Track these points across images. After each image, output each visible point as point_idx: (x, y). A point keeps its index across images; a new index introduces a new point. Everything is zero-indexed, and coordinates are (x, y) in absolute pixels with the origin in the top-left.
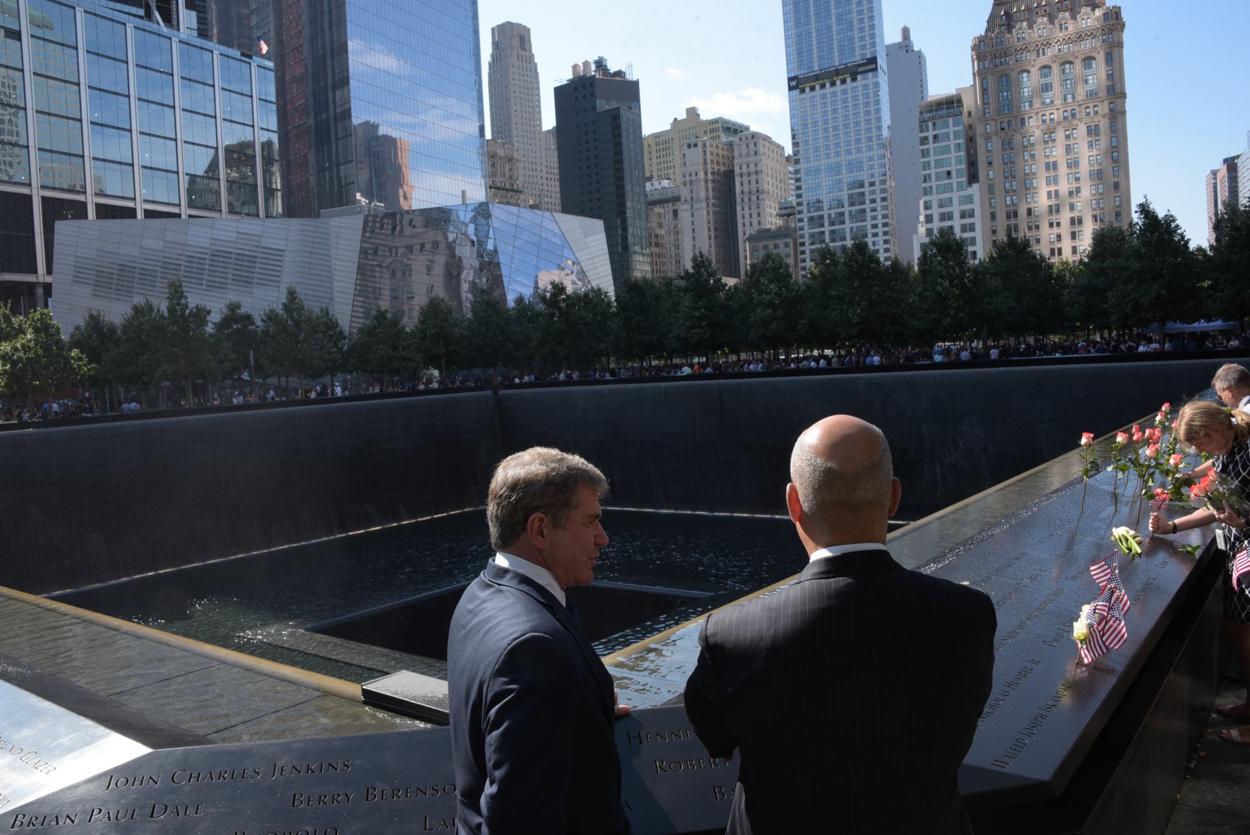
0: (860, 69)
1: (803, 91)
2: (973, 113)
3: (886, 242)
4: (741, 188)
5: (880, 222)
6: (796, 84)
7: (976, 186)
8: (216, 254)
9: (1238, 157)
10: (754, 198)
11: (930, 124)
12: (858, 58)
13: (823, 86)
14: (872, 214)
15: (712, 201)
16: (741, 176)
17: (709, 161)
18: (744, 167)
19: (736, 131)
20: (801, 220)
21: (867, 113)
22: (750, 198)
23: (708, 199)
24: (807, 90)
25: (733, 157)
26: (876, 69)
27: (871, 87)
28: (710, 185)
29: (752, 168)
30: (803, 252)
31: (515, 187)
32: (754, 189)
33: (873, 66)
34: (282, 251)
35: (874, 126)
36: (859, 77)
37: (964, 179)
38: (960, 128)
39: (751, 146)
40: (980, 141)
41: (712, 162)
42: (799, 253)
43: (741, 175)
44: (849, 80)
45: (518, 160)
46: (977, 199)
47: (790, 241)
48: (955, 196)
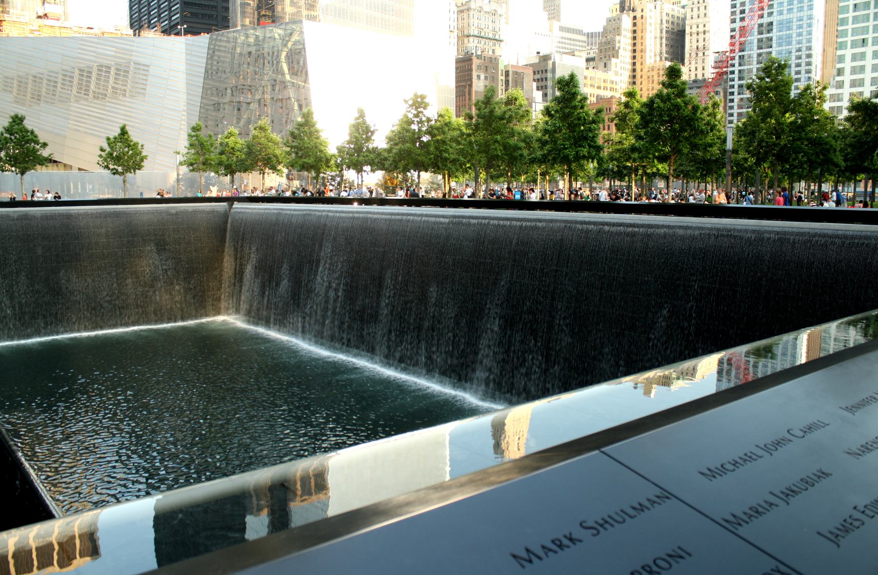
4: (690, 45)
8: (100, 67)
10: (700, 54)
14: (797, 69)
15: (665, 55)
16: (691, 35)
17: (664, 22)
18: (694, 27)
20: (733, 72)
22: (697, 54)
23: (661, 53)
28: (664, 40)
29: (701, 29)
30: (732, 101)
31: (497, 37)
32: (701, 45)
34: (148, 66)
39: (702, 8)
41: (667, 22)
42: (728, 101)
47: (720, 89)
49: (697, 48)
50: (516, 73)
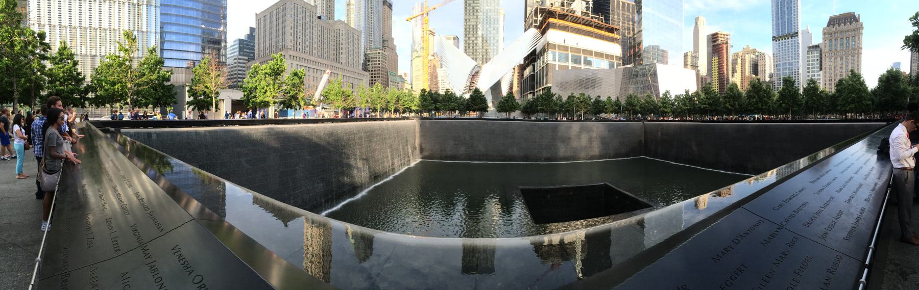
6: (774, 39)
7: (821, 71)
11: (810, 53)
13: (782, 40)
26: (798, 36)
36: (793, 38)
48: (816, 74)
50: (705, 79)
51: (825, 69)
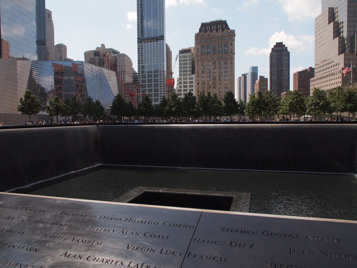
0: (159, 39)
1: (142, 43)
2: (194, 55)
3: (164, 89)
5: (162, 83)
7: (194, 75)
9: (247, 74)
10: (123, 73)
12: (158, 35)
13: (148, 42)
18: (120, 63)
19: (118, 53)
21: (160, 51)
22: (121, 73)
24: (143, 43)
25: (117, 60)
27: (162, 44)
30: (140, 90)
33: (163, 38)
35: (162, 55)
36: (158, 41)
37: (191, 73)
38: (191, 58)
40: (196, 62)
43: (119, 66)
44: (155, 41)
45: (49, 53)
46: (194, 78)
48: (188, 77)
49: (122, 71)
51: (198, 72)
